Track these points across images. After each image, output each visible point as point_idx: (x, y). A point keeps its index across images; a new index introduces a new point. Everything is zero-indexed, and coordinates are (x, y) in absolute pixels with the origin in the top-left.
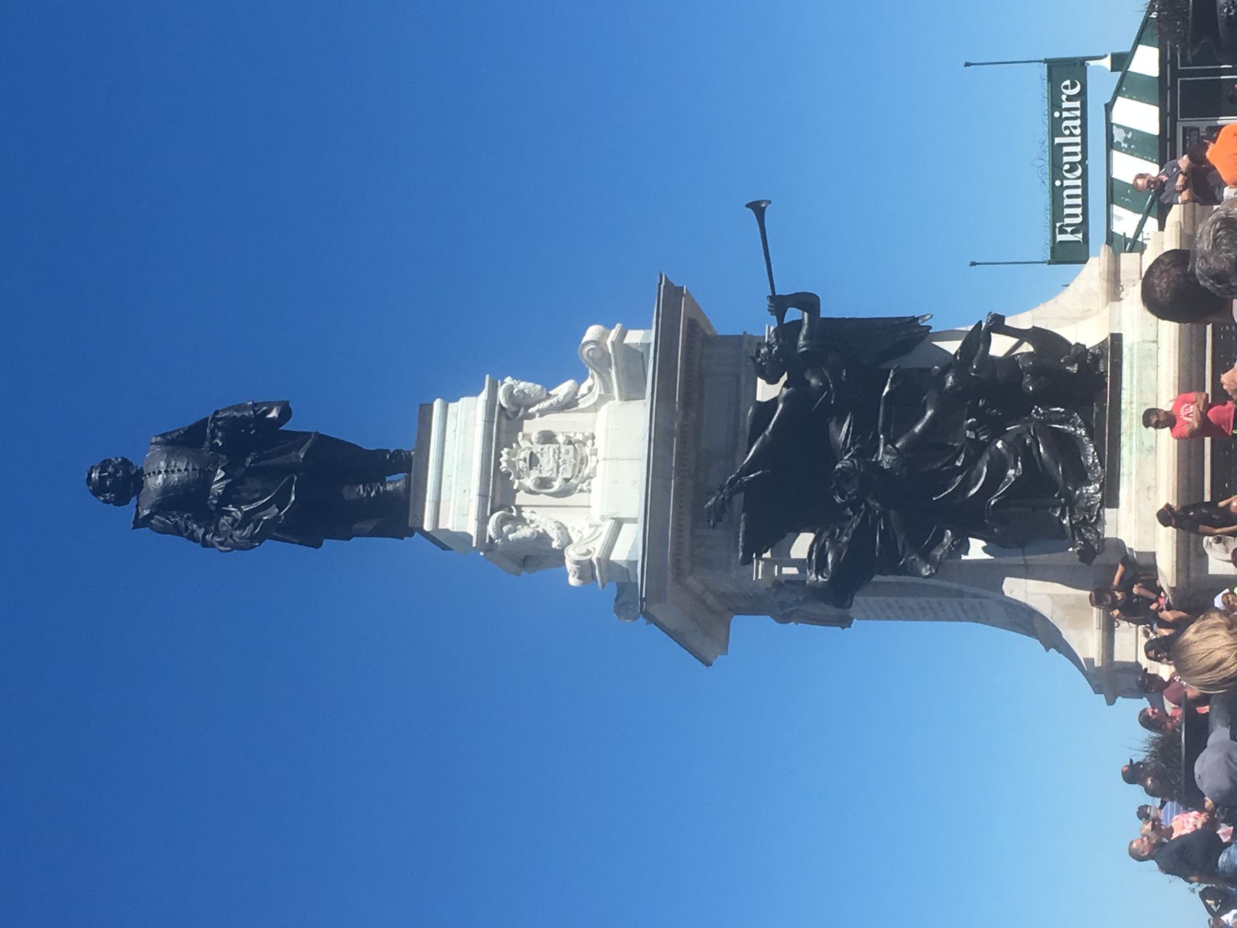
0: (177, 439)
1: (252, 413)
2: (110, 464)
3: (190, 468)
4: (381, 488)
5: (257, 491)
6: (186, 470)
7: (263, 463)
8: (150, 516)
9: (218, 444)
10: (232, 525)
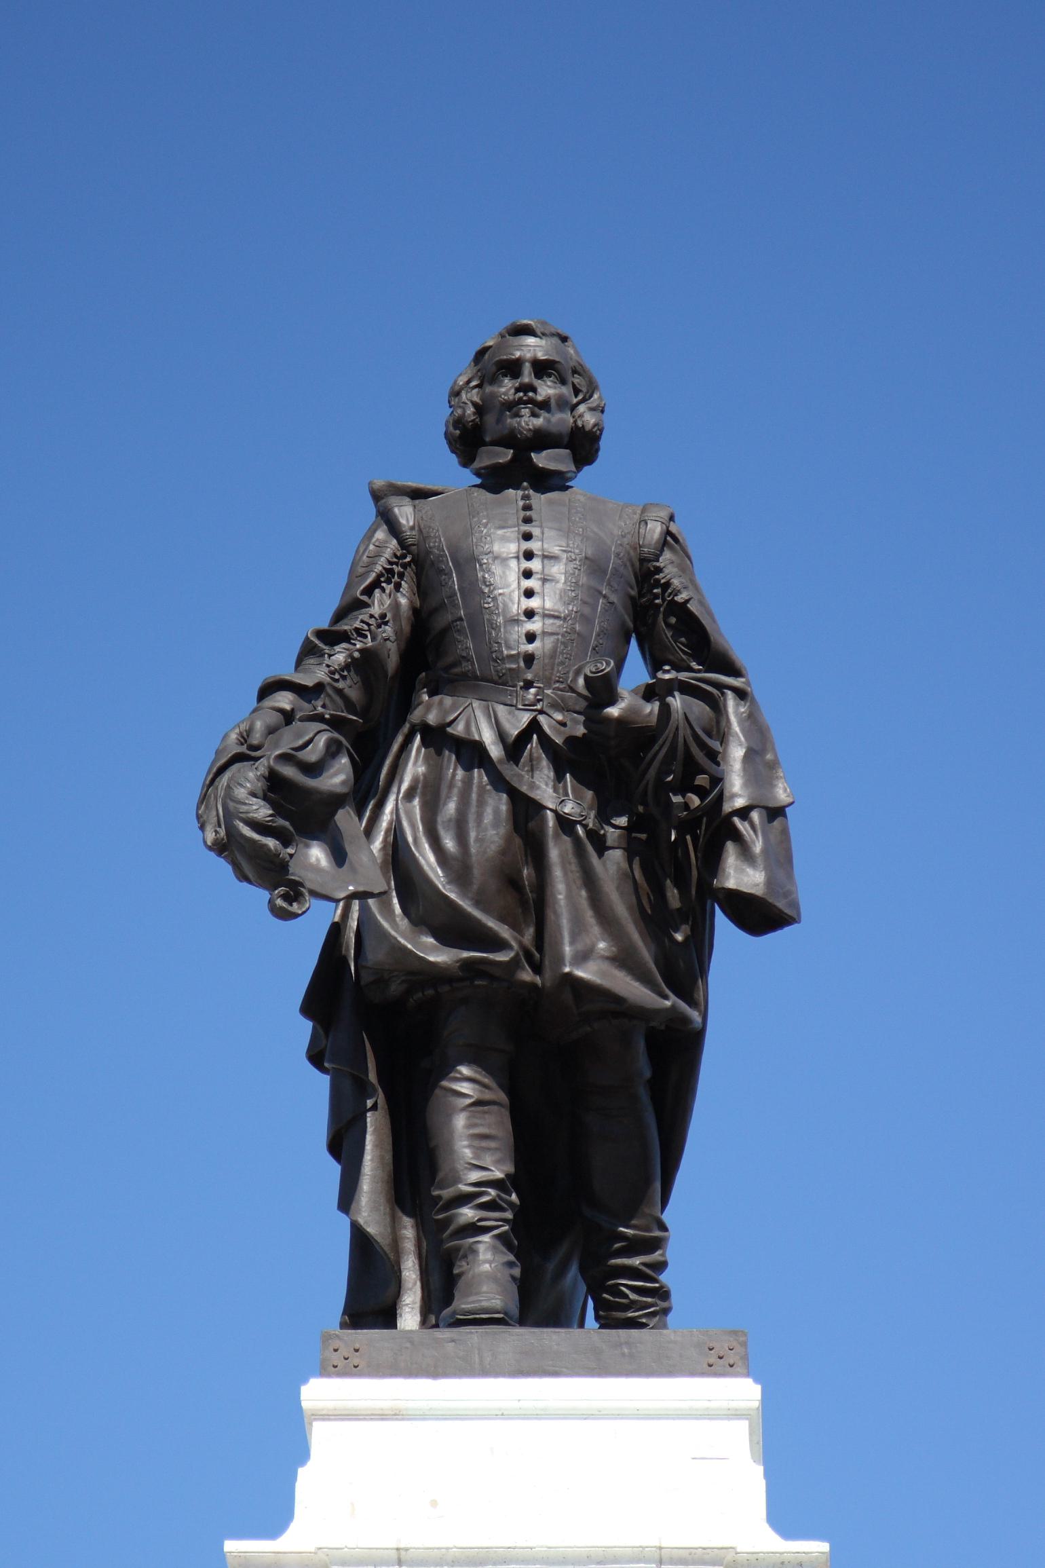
0: (657, 583)
1: (740, 803)
2: (576, 391)
3: (535, 626)
4: (486, 1238)
5: (462, 838)
6: (530, 614)
7: (557, 851)
8: (394, 529)
9: (612, 702)
10: (285, 758)
